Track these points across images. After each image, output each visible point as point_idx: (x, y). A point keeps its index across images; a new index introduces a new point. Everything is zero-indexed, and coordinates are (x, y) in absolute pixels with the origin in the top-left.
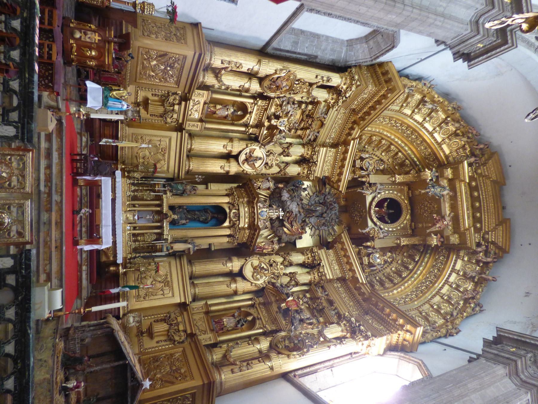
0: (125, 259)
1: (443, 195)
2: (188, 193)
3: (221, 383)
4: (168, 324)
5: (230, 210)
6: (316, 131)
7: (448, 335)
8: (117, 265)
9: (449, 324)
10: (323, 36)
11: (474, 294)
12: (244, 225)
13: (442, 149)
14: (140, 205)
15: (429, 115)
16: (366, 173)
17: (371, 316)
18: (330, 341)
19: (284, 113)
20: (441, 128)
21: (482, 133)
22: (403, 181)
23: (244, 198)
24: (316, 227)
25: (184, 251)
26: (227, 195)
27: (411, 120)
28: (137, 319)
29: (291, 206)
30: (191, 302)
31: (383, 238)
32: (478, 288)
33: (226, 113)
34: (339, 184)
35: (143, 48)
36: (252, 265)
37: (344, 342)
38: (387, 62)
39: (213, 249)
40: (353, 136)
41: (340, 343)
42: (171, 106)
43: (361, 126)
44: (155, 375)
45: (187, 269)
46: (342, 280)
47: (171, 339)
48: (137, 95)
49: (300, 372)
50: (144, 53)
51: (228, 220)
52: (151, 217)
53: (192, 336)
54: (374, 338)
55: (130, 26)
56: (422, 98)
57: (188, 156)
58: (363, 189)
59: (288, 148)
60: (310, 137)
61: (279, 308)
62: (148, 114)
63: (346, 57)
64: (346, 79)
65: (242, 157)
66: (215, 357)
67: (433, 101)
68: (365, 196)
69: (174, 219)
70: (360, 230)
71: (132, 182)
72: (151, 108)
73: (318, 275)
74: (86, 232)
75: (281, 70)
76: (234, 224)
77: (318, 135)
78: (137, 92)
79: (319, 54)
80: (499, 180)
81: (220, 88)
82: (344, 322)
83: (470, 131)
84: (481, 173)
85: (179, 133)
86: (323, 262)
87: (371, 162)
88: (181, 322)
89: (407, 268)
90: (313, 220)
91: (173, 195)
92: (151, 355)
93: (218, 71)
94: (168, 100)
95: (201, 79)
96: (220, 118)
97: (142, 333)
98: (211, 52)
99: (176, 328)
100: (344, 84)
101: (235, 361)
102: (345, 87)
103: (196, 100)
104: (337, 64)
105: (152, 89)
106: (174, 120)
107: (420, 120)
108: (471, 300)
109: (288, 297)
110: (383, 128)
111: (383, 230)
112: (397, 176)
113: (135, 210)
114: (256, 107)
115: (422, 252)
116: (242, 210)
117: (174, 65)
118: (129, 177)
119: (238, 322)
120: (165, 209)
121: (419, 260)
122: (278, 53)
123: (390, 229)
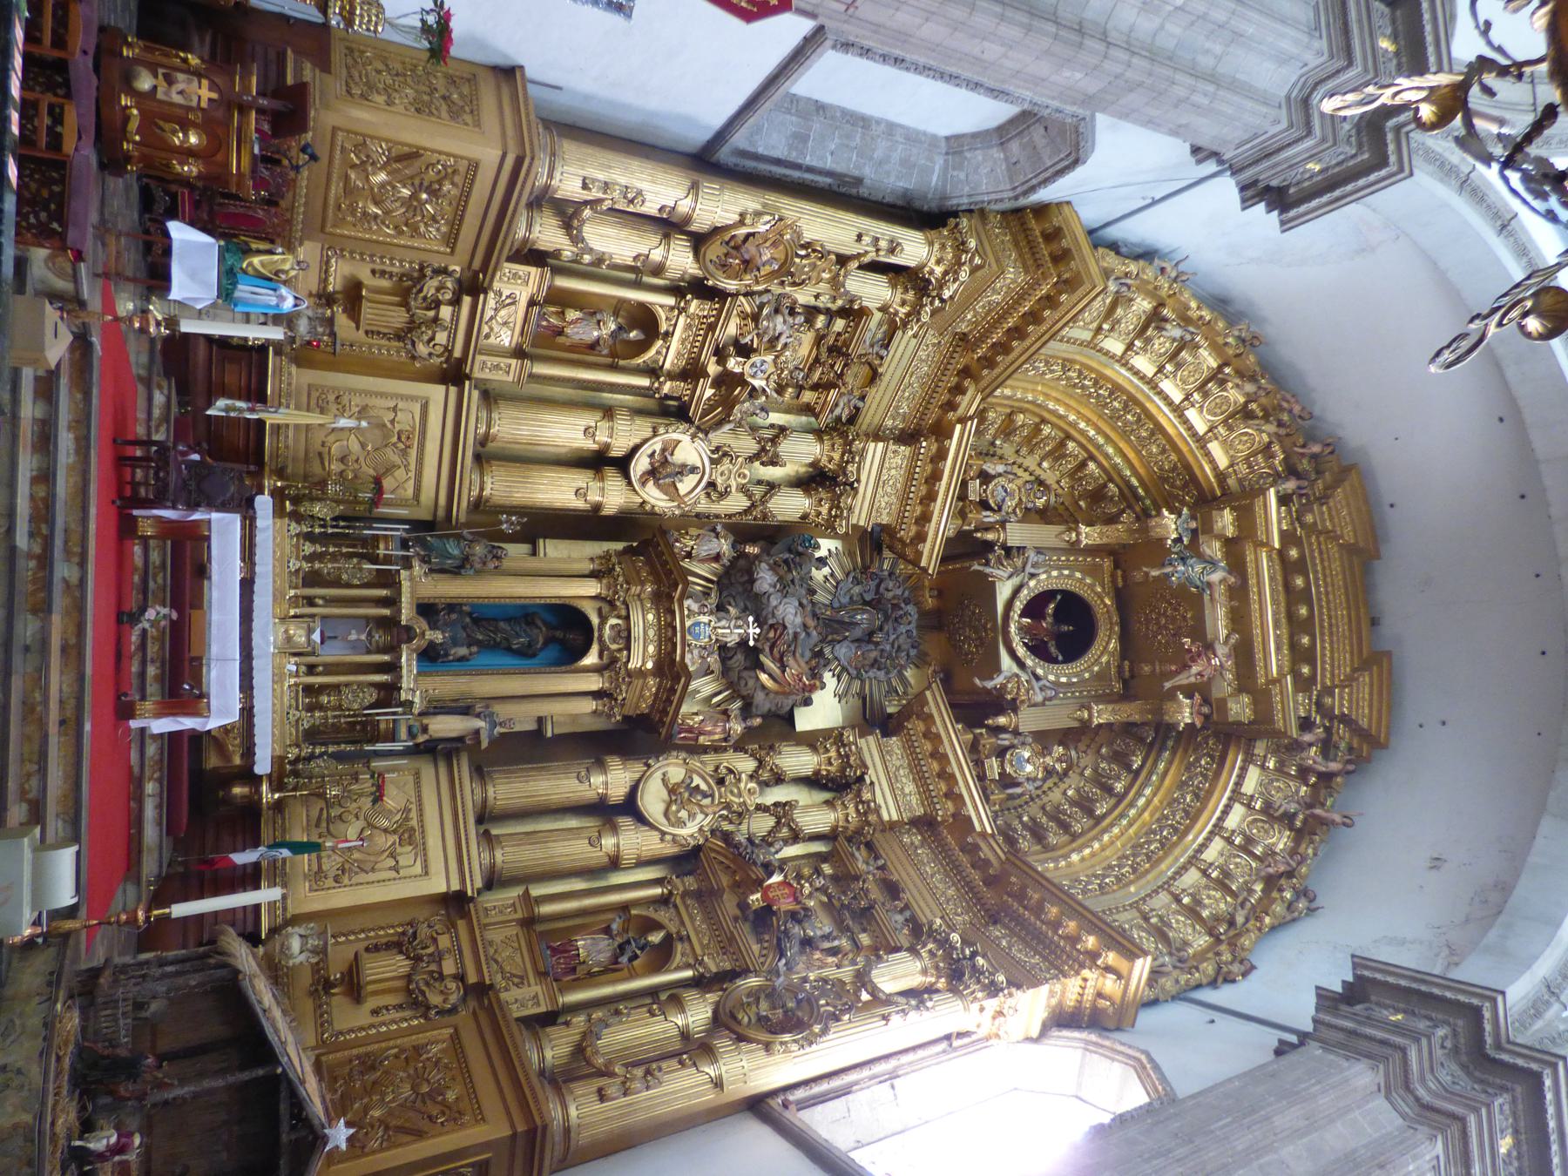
0: (278, 761)
1: (1209, 585)
2: (478, 566)
3: (567, 1131)
4: (408, 958)
5: (603, 619)
6: (857, 393)
7: (1220, 980)
8: (254, 780)
9: (1223, 947)
10: (878, 122)
11: (1294, 864)
12: (644, 663)
13: (1208, 454)
14: (330, 601)
15: (1173, 356)
16: (997, 517)
17: (1006, 927)
18: (888, 1001)
19: (766, 339)
20: (1206, 395)
21: (1317, 411)
22: (1098, 541)
23: (642, 584)
24: (854, 672)
25: (460, 739)
26: (594, 575)
27: (1123, 371)
28: (313, 942)
29: (781, 608)
30: (479, 892)
31: (1043, 704)
32: (1304, 846)
33: (596, 334)
34: (920, 547)
35: (348, 132)
36: (664, 781)
37: (929, 1004)
38: (1059, 204)
39: (549, 734)
40: (960, 411)
41: (917, 1008)
42: (428, 309)
43: (983, 383)
44: (366, 1110)
45: (470, 792)
46: (926, 824)
47: (417, 1003)
48: (326, 271)
49: (800, 1094)
50: (348, 146)
51: (595, 649)
52: (363, 637)
53: (481, 991)
54: (1013, 990)
55: (308, 66)
56: (1155, 308)
57: (478, 458)
58: (987, 564)
59: (774, 441)
60: (837, 411)
61: (743, 906)
62: (358, 328)
63: (944, 186)
64: (943, 247)
65: (640, 465)
66: (549, 1054)
67: (1185, 320)
68: (994, 582)
69: (432, 644)
70: (977, 681)
71: (305, 529)
72: (367, 311)
73: (857, 810)
74: (160, 679)
75: (758, 214)
76: (614, 660)
77: (860, 404)
78: (328, 262)
79: (868, 172)
80: (1361, 544)
81: (576, 260)
82: (930, 946)
83: (1285, 405)
84: (1315, 523)
85: (453, 390)
86: (871, 771)
87: (1010, 487)
88: (449, 951)
89: (1109, 790)
90: (844, 650)
91: (431, 571)
92: (355, 1052)
93: (571, 211)
94: (421, 290)
95: (521, 232)
96: (573, 348)
97: (328, 985)
98: (553, 154)
99: (433, 967)
100: (938, 262)
101: (609, 1063)
102: (939, 270)
103: (506, 293)
104: (917, 204)
105: (372, 256)
106: (439, 350)
107: (1148, 369)
108: (1283, 881)
109: (770, 875)
110: (1045, 390)
111: (1042, 683)
112: (1083, 529)
113: (312, 616)
114: (682, 319)
115: (1151, 745)
116: (637, 618)
117: (441, 185)
118: (296, 517)
119: (622, 948)
120: (407, 613)
121: (1141, 767)
122: (750, 164)
123: (1064, 680)
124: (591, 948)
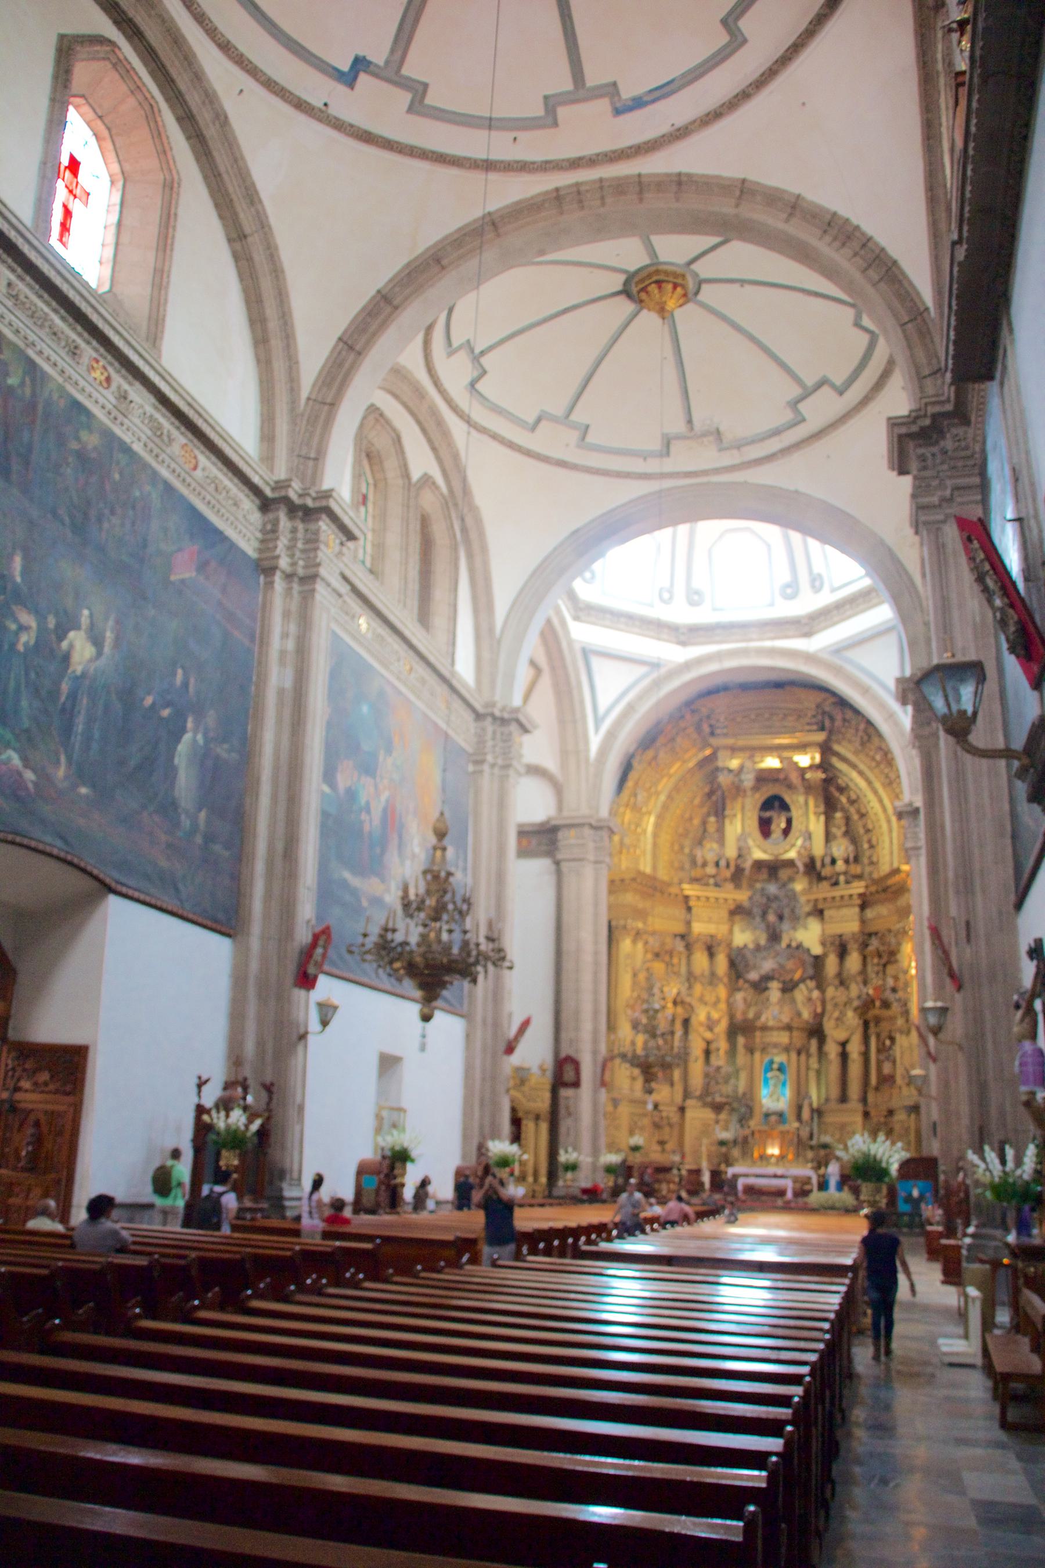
65: (708, 1035)
72: (666, 1138)
112: (727, 812)
116: (768, 1040)
124: (887, 1069)
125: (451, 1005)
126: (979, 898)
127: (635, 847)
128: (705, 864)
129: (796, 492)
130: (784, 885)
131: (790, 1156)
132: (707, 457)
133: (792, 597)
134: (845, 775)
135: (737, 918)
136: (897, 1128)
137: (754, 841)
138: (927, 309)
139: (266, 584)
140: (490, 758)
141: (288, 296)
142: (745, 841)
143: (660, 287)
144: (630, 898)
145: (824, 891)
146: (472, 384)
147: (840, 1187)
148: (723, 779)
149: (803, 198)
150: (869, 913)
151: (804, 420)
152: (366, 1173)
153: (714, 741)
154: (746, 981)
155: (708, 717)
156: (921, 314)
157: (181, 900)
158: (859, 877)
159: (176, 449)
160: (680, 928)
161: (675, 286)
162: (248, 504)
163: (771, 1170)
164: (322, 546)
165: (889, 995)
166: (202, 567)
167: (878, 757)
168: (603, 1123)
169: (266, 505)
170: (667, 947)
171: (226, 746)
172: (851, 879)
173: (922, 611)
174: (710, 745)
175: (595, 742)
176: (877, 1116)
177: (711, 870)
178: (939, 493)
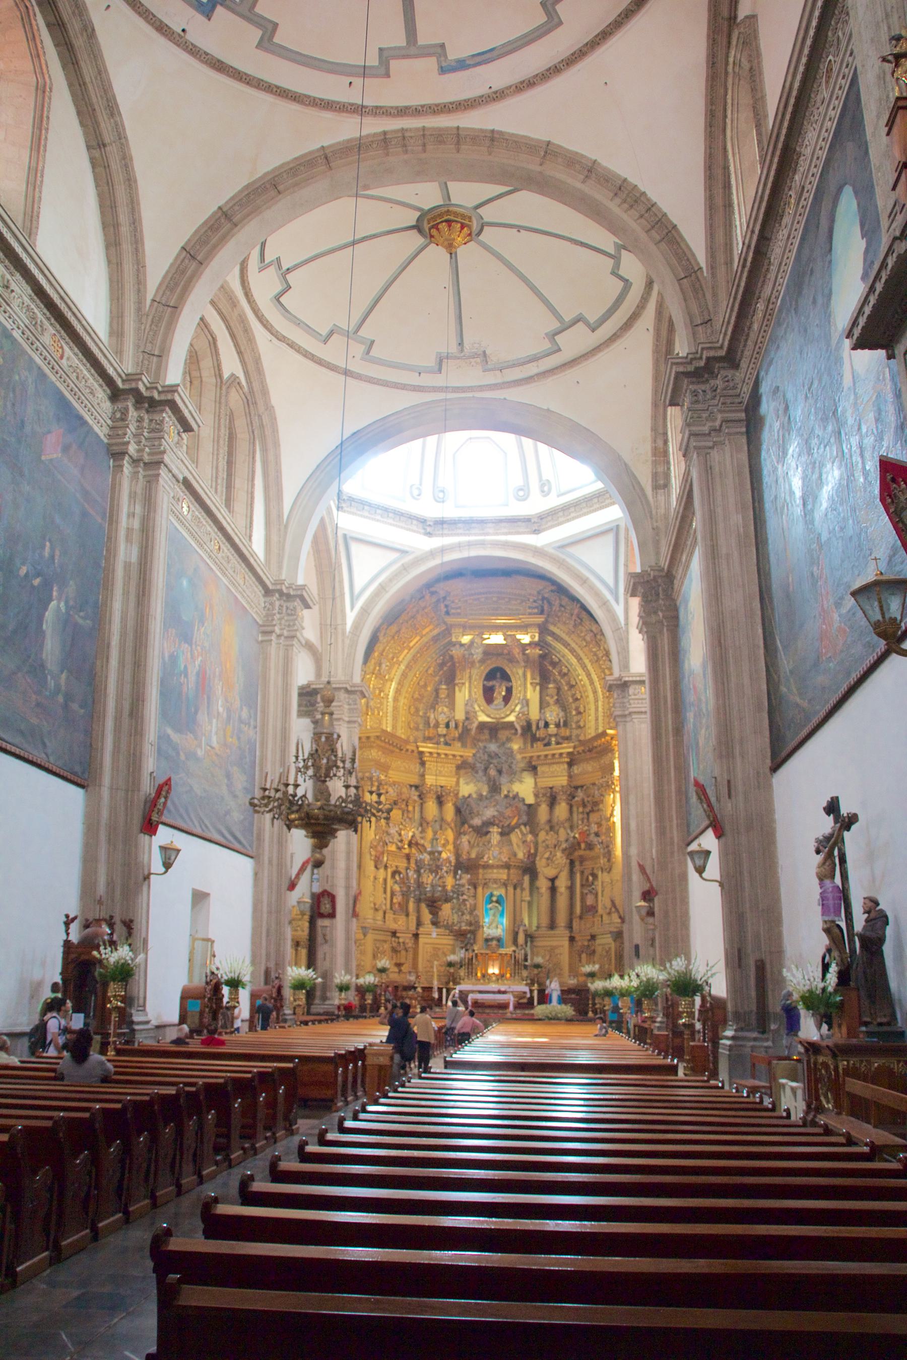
26: (475, 888)
40: (414, 748)
58: (470, 730)
72: (403, 961)
89: (565, 674)
112: (457, 681)
116: (488, 876)
124: (590, 900)
125: (244, 846)
126: (738, 760)
127: (378, 709)
128: (437, 725)
129: (548, 410)
130: (503, 744)
131: (508, 975)
132: (472, 376)
133: (524, 499)
134: (559, 652)
135: (462, 772)
136: (599, 950)
137: (479, 706)
138: (701, 268)
139: (114, 466)
140: (277, 630)
141: (139, 204)
142: (472, 706)
143: (450, 226)
144: (374, 754)
145: (538, 750)
146: (277, 298)
147: (563, 1000)
148: (456, 652)
149: (599, 164)
150: (576, 770)
151: (559, 350)
152: (189, 998)
153: (450, 620)
154: (471, 826)
155: (445, 598)
156: (695, 272)
157: (46, 754)
158: (568, 739)
159: (47, 339)
160: (415, 780)
161: (462, 227)
162: (101, 394)
163: (494, 987)
164: (166, 436)
165: (592, 837)
166: (66, 449)
167: (588, 638)
168: (354, 948)
169: (115, 395)
170: (404, 797)
171: (82, 614)
172: (560, 741)
173: (651, 518)
174: (445, 623)
175: (351, 617)
176: (581, 941)
177: (442, 730)
178: (709, 424)
